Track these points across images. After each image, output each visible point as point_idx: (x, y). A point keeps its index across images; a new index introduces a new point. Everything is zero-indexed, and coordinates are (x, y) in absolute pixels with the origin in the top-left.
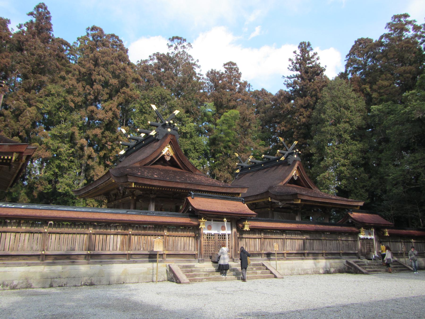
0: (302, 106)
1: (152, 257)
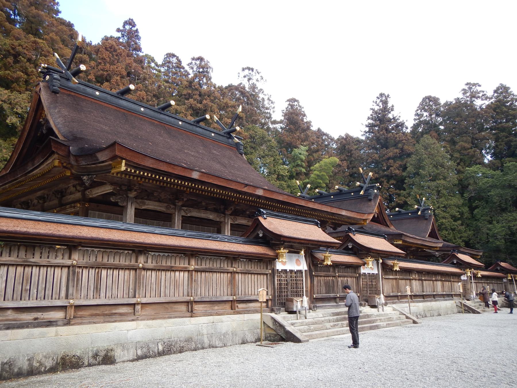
0: (389, 159)
1: (450, 296)
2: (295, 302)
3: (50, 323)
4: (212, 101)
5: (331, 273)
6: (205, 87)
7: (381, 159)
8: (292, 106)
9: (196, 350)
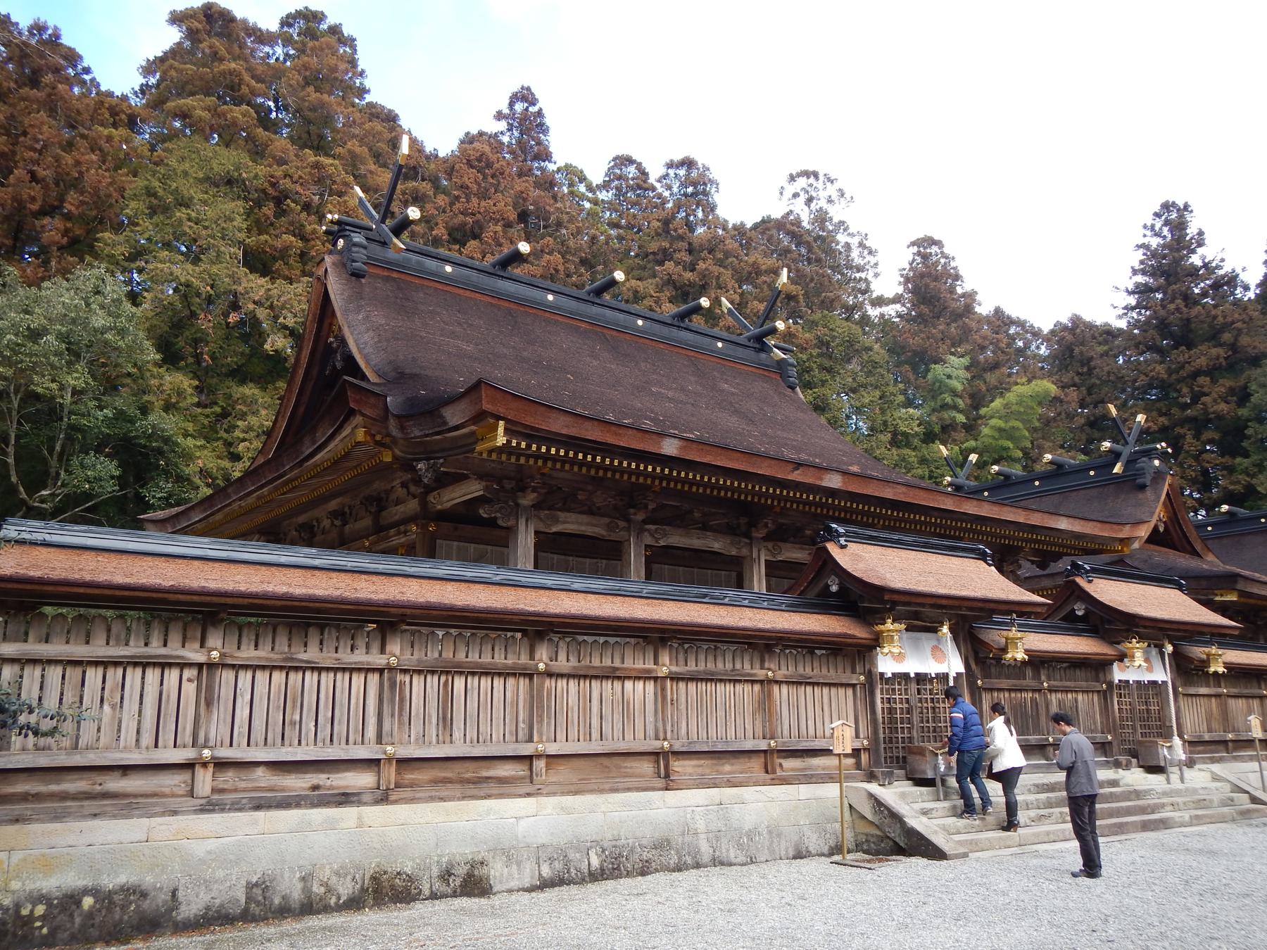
0: (1196, 374)
2: (929, 757)
3: (345, 798)
4: (720, 263)
5: (1029, 682)
6: (700, 230)
7: (1174, 376)
8: (925, 257)
9: (680, 870)
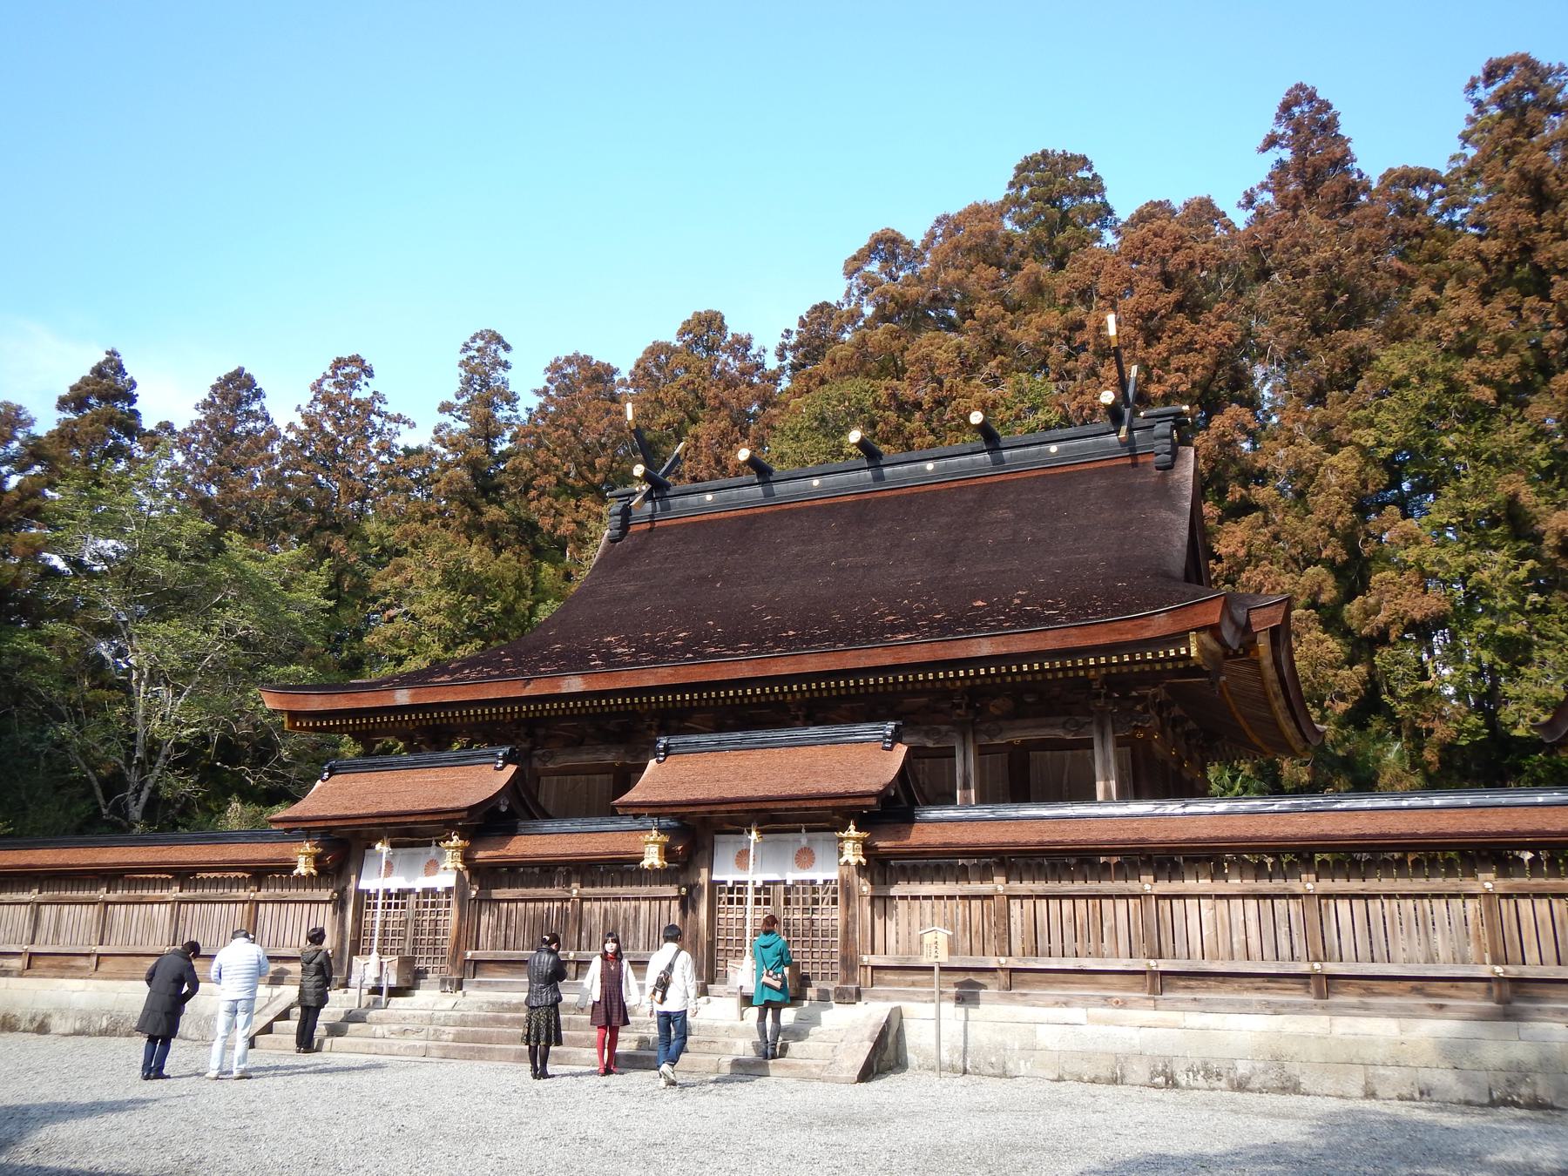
5: (555, 891)
